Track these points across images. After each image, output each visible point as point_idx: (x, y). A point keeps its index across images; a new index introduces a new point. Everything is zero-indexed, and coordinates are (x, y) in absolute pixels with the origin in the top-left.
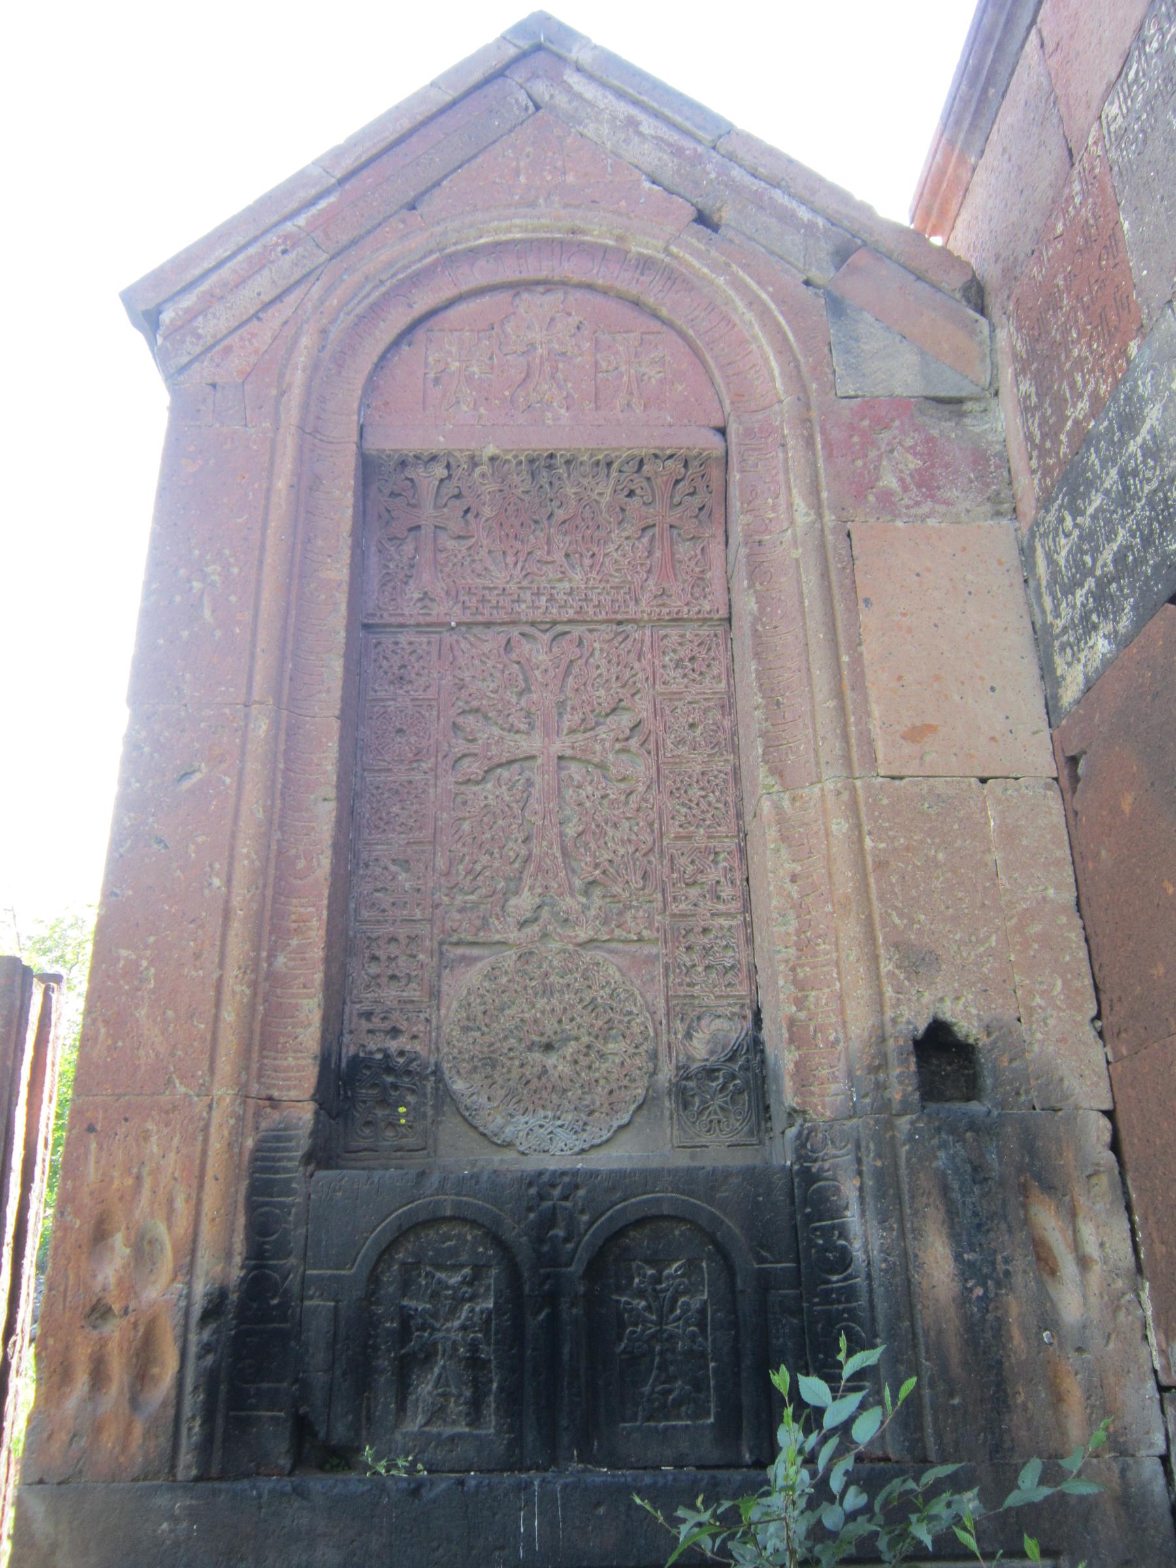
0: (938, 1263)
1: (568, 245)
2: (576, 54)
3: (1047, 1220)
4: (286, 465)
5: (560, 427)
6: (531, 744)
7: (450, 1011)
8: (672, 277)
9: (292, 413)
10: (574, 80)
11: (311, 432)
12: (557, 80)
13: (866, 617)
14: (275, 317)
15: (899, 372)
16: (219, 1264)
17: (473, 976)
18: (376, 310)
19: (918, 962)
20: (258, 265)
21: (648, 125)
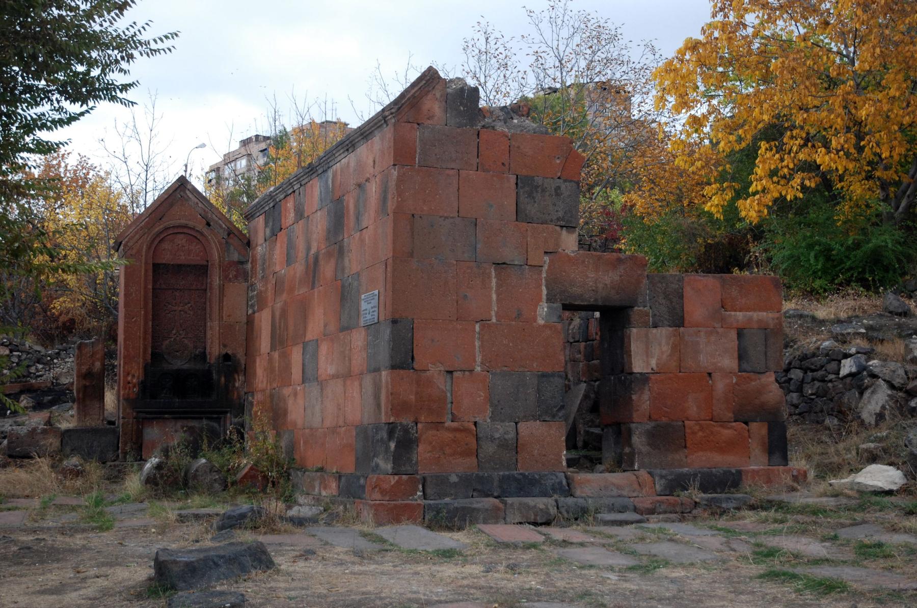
0: (223, 379)
1: (186, 227)
2: (189, 187)
3: (236, 376)
4: (143, 271)
5: (182, 259)
6: (176, 308)
7: (164, 347)
8: (202, 234)
9: (143, 261)
10: (188, 192)
11: (146, 263)
12: (185, 192)
13: (225, 299)
14: (140, 242)
15: (235, 257)
16: (141, 378)
17: (167, 342)
18: (154, 239)
19: (225, 346)
20: (137, 233)
21: (200, 205)
